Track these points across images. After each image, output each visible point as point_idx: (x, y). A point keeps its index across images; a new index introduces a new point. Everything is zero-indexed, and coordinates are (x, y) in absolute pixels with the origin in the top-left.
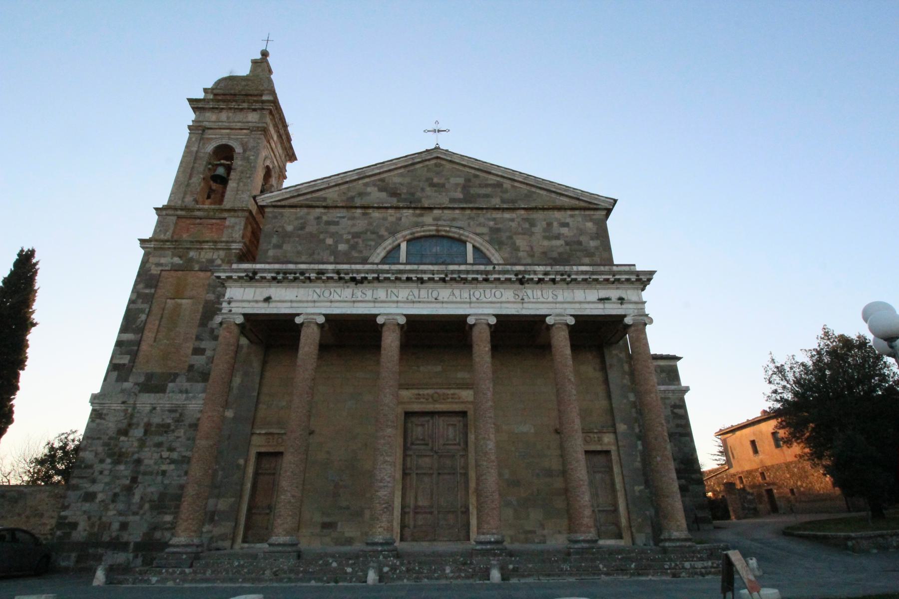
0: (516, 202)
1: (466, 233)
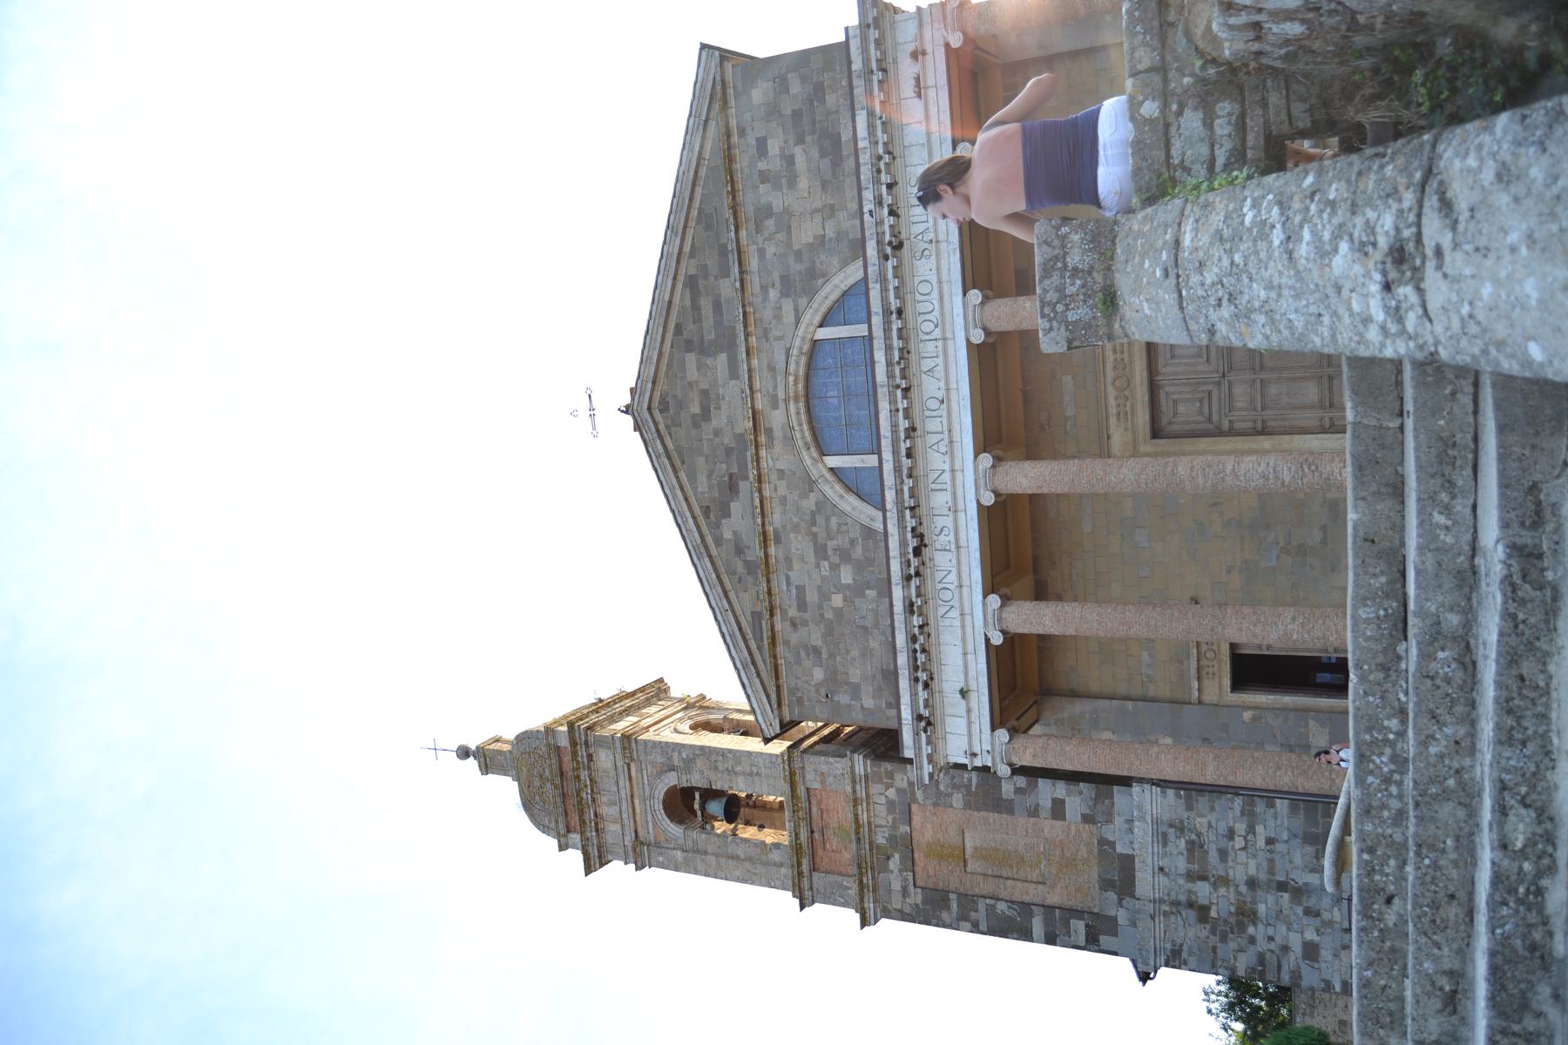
0: (725, 246)
1: (798, 342)
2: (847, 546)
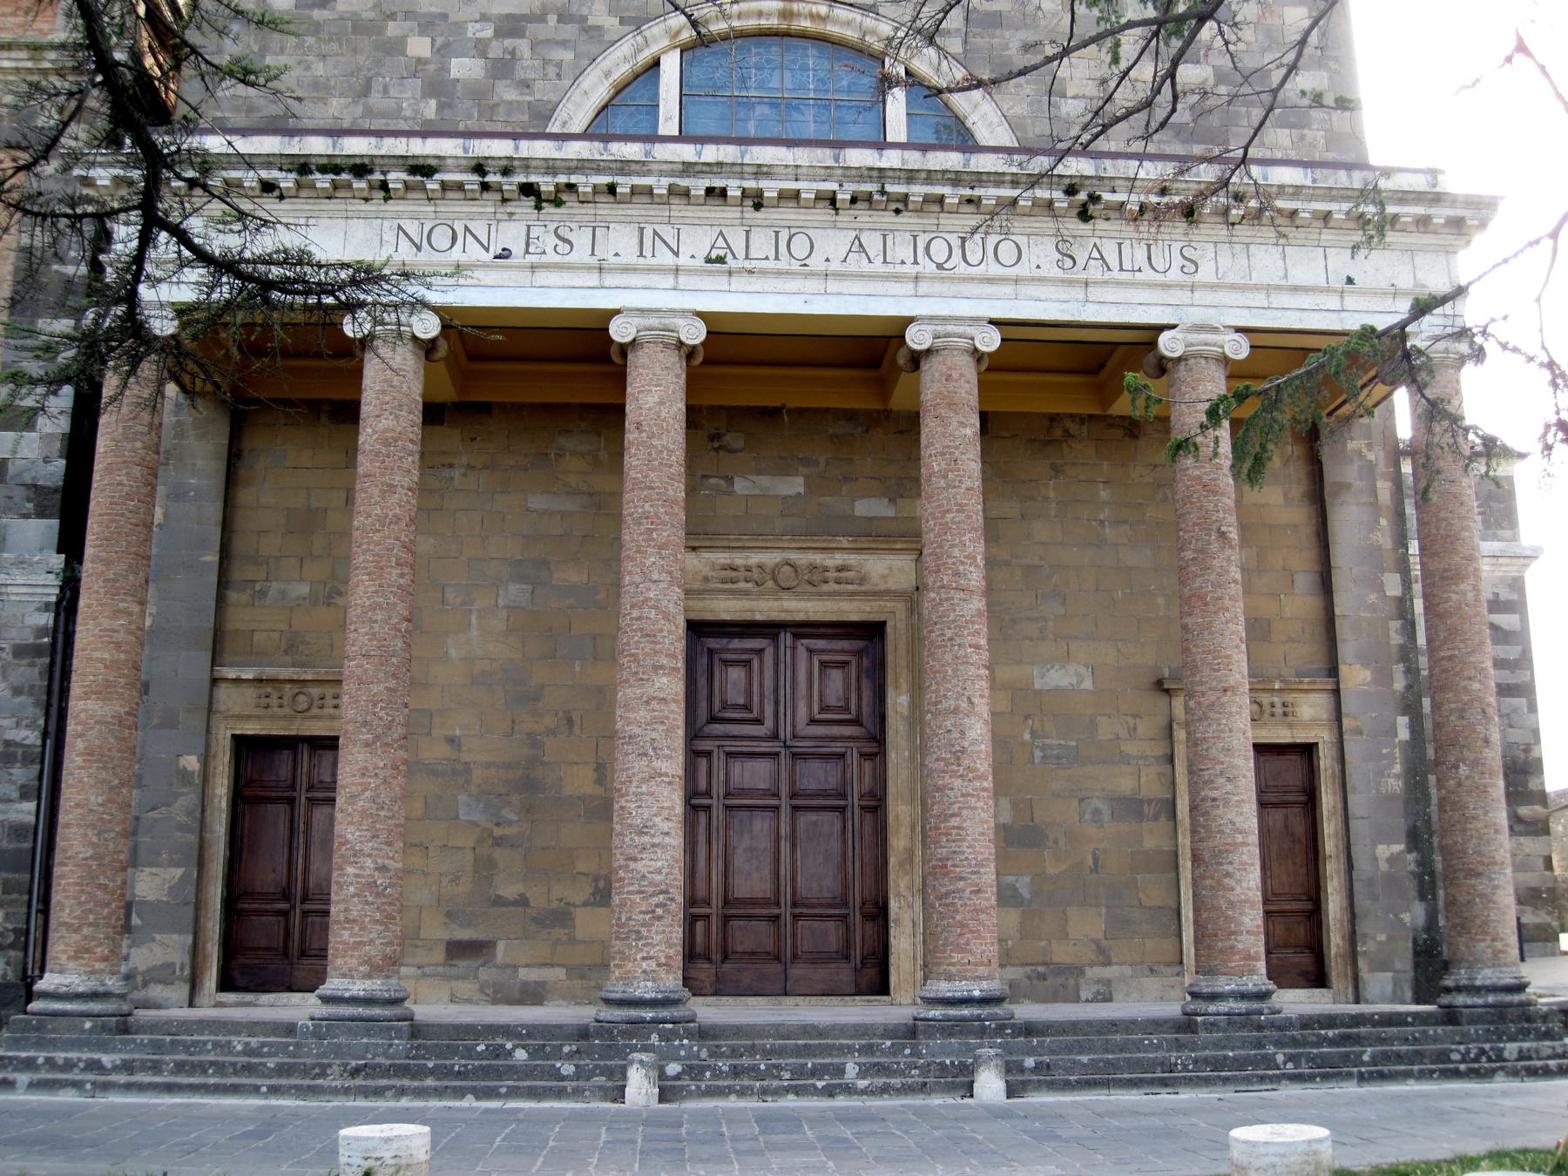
2: (520, 74)
